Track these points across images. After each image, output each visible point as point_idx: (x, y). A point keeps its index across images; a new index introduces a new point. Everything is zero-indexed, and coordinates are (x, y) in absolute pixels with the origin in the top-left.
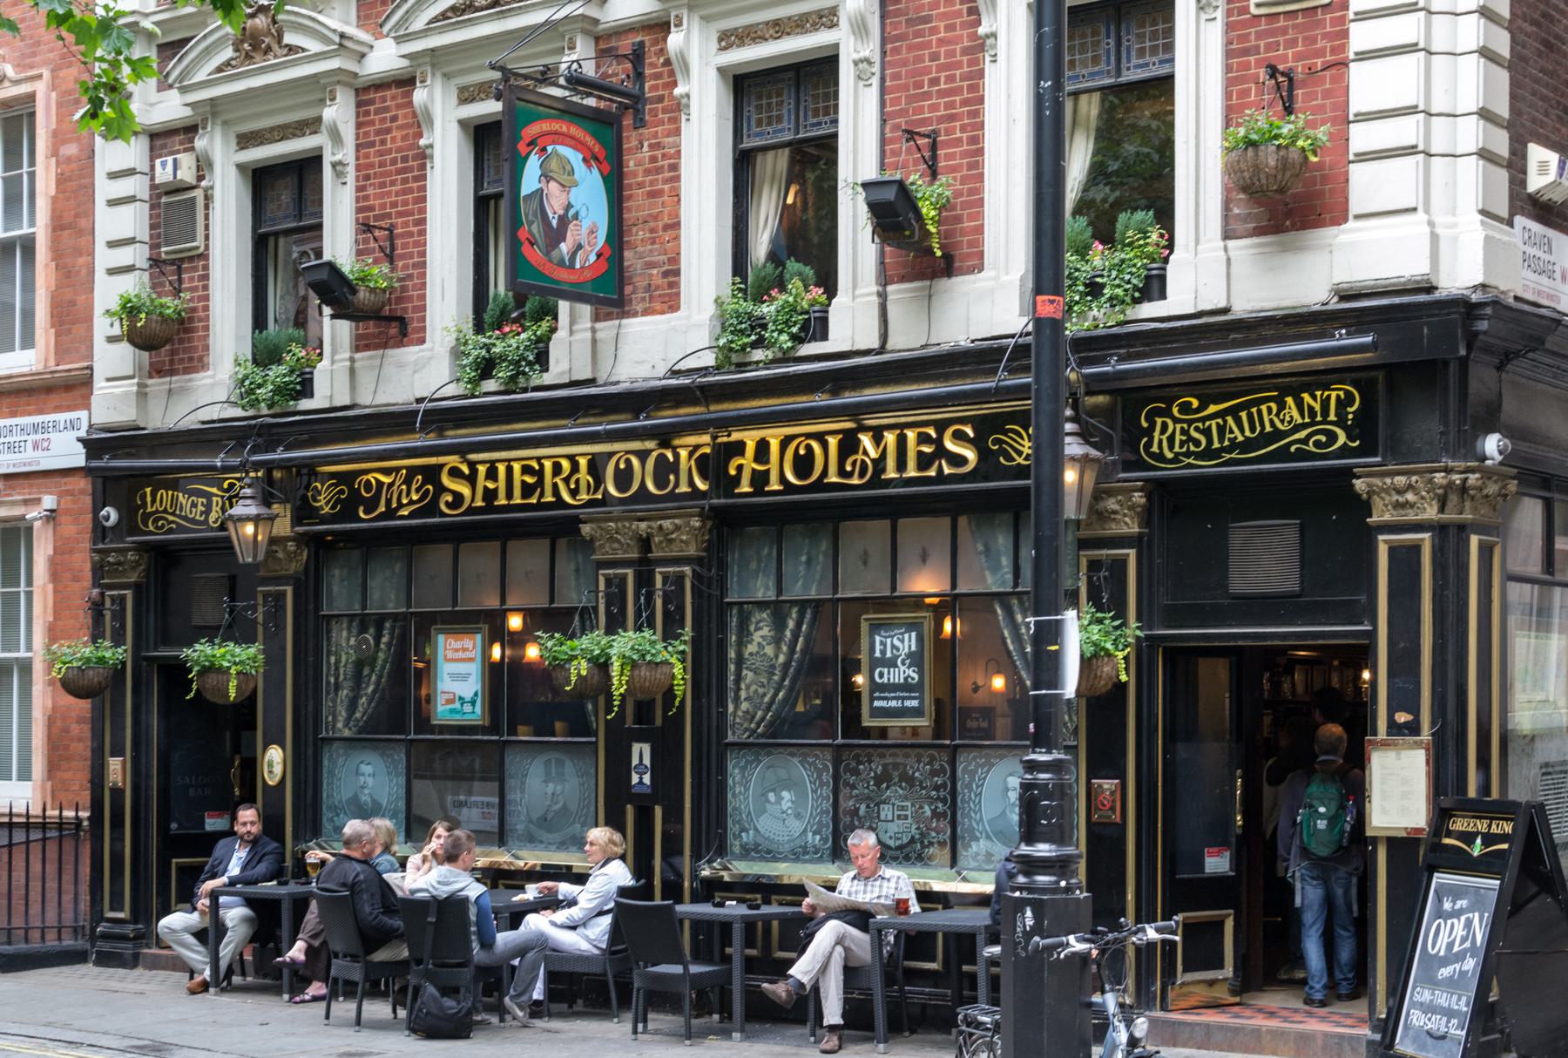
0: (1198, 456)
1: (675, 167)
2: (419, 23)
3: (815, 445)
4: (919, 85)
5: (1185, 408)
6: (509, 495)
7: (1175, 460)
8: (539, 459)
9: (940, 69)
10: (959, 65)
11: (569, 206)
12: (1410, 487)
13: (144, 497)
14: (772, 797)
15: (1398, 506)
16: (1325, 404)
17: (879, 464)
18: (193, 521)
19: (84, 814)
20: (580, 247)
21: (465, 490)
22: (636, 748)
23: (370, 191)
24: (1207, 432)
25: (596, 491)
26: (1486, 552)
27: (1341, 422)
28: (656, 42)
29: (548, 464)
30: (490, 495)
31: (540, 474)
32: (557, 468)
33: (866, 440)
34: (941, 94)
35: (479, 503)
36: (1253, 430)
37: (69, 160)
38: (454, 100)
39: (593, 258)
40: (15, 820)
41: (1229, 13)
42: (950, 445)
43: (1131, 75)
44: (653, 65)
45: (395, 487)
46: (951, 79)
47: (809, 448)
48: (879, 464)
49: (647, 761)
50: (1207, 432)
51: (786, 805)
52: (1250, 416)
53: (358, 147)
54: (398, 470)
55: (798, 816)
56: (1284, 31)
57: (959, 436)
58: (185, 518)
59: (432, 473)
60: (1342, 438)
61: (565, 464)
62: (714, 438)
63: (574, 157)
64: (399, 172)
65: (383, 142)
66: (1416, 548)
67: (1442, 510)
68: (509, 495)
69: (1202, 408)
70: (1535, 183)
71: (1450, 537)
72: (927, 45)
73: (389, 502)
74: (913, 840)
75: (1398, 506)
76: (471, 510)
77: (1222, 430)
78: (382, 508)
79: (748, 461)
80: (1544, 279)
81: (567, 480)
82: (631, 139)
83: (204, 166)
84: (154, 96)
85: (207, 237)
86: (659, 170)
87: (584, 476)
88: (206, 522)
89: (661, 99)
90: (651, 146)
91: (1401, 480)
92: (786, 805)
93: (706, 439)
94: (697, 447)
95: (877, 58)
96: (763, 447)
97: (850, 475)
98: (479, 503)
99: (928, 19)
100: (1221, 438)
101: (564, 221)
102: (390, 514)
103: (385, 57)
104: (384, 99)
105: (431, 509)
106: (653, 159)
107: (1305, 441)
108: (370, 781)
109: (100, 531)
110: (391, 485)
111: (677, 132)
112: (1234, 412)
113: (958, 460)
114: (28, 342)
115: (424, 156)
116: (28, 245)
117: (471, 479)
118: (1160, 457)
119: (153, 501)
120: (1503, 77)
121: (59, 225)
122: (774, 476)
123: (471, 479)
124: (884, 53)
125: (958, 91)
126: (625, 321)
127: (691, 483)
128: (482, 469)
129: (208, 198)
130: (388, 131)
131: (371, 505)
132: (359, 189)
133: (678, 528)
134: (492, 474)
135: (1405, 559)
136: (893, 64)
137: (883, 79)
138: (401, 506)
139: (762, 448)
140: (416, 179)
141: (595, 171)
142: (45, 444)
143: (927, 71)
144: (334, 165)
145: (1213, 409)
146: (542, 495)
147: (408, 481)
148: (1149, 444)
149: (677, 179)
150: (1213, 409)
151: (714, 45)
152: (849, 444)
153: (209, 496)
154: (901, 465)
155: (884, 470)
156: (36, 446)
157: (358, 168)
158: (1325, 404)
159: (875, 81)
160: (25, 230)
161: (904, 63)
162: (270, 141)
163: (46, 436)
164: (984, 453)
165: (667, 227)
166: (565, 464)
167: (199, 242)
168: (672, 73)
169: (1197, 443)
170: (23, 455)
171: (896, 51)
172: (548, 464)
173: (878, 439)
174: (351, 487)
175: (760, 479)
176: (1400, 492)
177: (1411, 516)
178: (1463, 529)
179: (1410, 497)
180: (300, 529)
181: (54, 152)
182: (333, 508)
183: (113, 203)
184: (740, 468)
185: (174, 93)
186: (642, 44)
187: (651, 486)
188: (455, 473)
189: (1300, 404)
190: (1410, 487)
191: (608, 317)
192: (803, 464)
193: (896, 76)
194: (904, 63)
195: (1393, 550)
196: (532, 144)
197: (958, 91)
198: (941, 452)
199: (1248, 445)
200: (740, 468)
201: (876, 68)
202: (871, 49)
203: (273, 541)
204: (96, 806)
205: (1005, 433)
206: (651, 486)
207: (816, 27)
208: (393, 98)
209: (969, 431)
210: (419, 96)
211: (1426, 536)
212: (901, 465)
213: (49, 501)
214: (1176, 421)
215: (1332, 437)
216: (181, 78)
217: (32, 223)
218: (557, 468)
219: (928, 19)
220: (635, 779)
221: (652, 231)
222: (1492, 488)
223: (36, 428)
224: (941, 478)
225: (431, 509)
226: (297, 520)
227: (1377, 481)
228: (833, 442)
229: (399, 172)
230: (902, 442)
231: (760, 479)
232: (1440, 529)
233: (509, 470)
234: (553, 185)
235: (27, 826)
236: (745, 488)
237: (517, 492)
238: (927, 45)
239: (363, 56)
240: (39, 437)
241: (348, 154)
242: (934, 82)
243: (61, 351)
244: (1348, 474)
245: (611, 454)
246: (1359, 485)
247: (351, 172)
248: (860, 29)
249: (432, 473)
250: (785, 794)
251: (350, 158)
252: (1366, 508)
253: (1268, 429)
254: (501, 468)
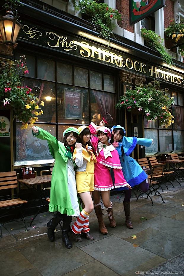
6: (102, 58)
22: (135, 128)
25: (124, 65)
45: (63, 41)
49: (137, 131)
73: (60, 44)
78: (57, 45)
98: (93, 56)
110: (61, 40)
174: (44, 34)
182: (35, 37)
184: (151, 71)
200: (151, 71)
224: (177, 84)
236: (152, 75)
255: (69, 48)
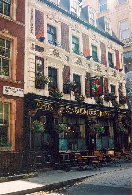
13: (37, 104)
21: (77, 111)
30: (80, 112)
31: (84, 110)
35: (78, 113)
58: (44, 108)
59: (74, 109)
98: (78, 113)
102: (69, 112)
105: (74, 112)
117: (78, 110)
119: (38, 105)
123: (78, 110)
131: (68, 111)
134: (80, 110)
138: (71, 112)
142: (15, 92)
147: (72, 109)
153: (47, 106)
163: (16, 91)
164: (112, 115)
170: (11, 93)
225: (74, 113)
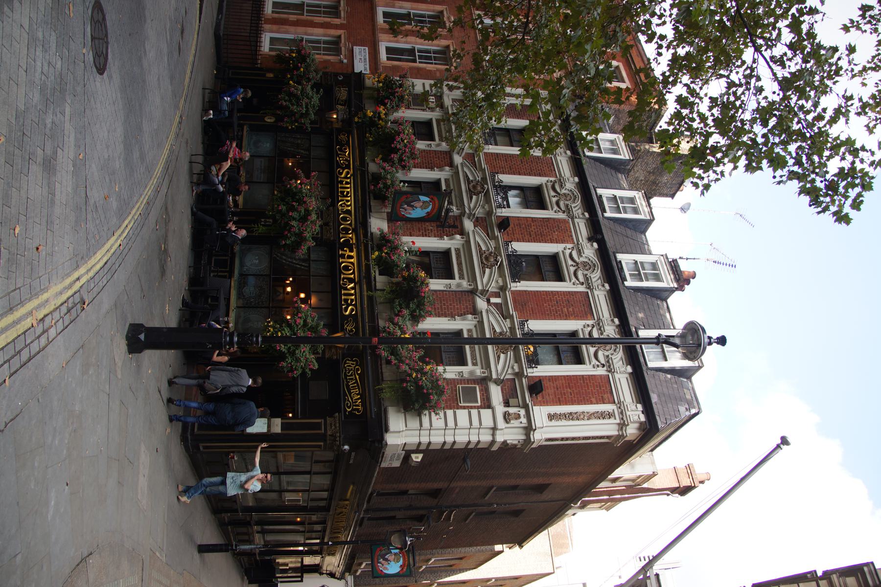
0: (345, 373)
1: (426, 236)
2: (466, 169)
3: (351, 271)
4: (444, 300)
5: (358, 370)
6: (341, 188)
7: (344, 367)
8: (351, 196)
9: (447, 306)
10: (448, 311)
11: (416, 208)
12: (336, 427)
13: (345, 87)
14: (257, 257)
15: (331, 424)
16: (358, 406)
17: (346, 289)
18: (338, 101)
19: (259, 66)
20: (406, 210)
21: (343, 176)
23: (423, 154)
24: (351, 375)
26: (320, 446)
27: (353, 410)
28: (458, 231)
29: (349, 198)
31: (347, 196)
32: (348, 201)
33: (352, 285)
34: (441, 306)
36: (352, 387)
37: (435, 74)
38: (446, 177)
39: (403, 213)
40: (258, 43)
41: (457, 379)
42: (350, 308)
43: (444, 355)
44: (452, 231)
46: (445, 309)
47: (350, 270)
48: (346, 289)
50: (351, 375)
51: (255, 261)
52: (355, 386)
53: (435, 151)
54: (350, 157)
55: (251, 265)
56: (452, 393)
57: (352, 310)
59: (348, 167)
60: (348, 410)
61: (349, 203)
62: (354, 244)
63: (429, 209)
64: (428, 162)
65: (436, 158)
66: (320, 429)
67: (330, 435)
68: (341, 188)
69: (358, 374)
70: (413, 456)
71: (323, 437)
72: (454, 303)
74: (244, 296)
75: (331, 424)
76: (338, 177)
77: (352, 379)
79: (348, 253)
80: (389, 459)
81: (344, 203)
82: (434, 224)
83: (432, 110)
84: (451, 98)
85: (414, 109)
86: (425, 231)
87: (346, 208)
88: (338, 104)
89: (444, 232)
90: (431, 230)
91: (338, 425)
92: (255, 261)
93: (354, 242)
94: (352, 239)
95: (451, 289)
96: (352, 257)
97: (343, 281)
99: (460, 303)
100: (349, 379)
101: (412, 206)
103: (458, 159)
104: (447, 158)
106: (428, 230)
107: (348, 401)
108: (265, 146)
109: (336, 75)
111: (435, 237)
112: (357, 382)
113: (346, 310)
114: (388, 59)
115: (432, 169)
116: (414, 61)
117: (346, 177)
118: (345, 363)
120: (439, 447)
121: (419, 69)
122: (344, 260)
123: (346, 177)
124: (452, 291)
125: (442, 311)
126: (386, 221)
127: (342, 238)
128: (349, 180)
129: (424, 110)
130: (439, 160)
131: (340, 149)
132: (424, 150)
133: (331, 233)
135: (317, 426)
136: (449, 294)
137: (445, 291)
139: (351, 257)
140: (426, 166)
141: (425, 215)
143: (447, 303)
144: (431, 144)
145: (357, 377)
146: (341, 197)
147: (346, 160)
148: (349, 360)
149: (423, 236)
150: (357, 377)
151: (456, 247)
152: (351, 281)
154: (345, 295)
155: (344, 290)
156: (361, 59)
157: (430, 151)
158: (358, 406)
159: (445, 289)
160: (418, 60)
161: (450, 297)
162: (437, 127)
165: (410, 233)
166: (349, 203)
167: (412, 107)
168: (450, 236)
169: (349, 373)
171: (453, 295)
172: (349, 198)
173: (352, 288)
175: (343, 256)
176: (335, 425)
177: (328, 428)
178: (325, 441)
179: (333, 427)
180: (334, 130)
181: (438, 70)
183: (424, 84)
184: (346, 251)
185: (451, 103)
186: (458, 228)
187: (342, 226)
188: (348, 173)
189: (358, 399)
190: (336, 427)
191: (388, 216)
192: (346, 268)
193: (446, 294)
194: (450, 297)
195: (320, 424)
196: (432, 199)
197: (442, 311)
198: (348, 305)
199: (348, 386)
200: (346, 251)
201: (448, 289)
202: (454, 288)
203: (332, 122)
204: (261, 69)
205: (353, 323)
206: (342, 226)
207: (459, 274)
208: (447, 161)
209: (354, 313)
210: (447, 168)
211: (323, 431)
212: (345, 295)
213: (345, 61)
214: (355, 367)
215: (349, 408)
216: (454, 105)
217: (420, 62)
218: (348, 201)
219: (460, 303)
220: (263, 220)
221: (410, 229)
222: (335, 448)
223: (365, 59)
225: (339, 166)
226: (337, 129)
227: (337, 419)
228: (352, 276)
229: (428, 162)
230: (352, 295)
231: (343, 256)
232: (325, 435)
233: (348, 188)
234: (422, 204)
235: (256, 51)
237: (342, 190)
238: (454, 303)
239: (458, 154)
240: (363, 60)
241: (434, 148)
242: (444, 304)
243: (385, 68)
244: (340, 412)
245: (351, 216)
246: (337, 414)
247: (429, 149)
248: (459, 285)
249: (348, 167)
250: (257, 261)
251: (432, 149)
252: (331, 416)
253: (352, 391)
254: (349, 186)
255: (340, 161)
